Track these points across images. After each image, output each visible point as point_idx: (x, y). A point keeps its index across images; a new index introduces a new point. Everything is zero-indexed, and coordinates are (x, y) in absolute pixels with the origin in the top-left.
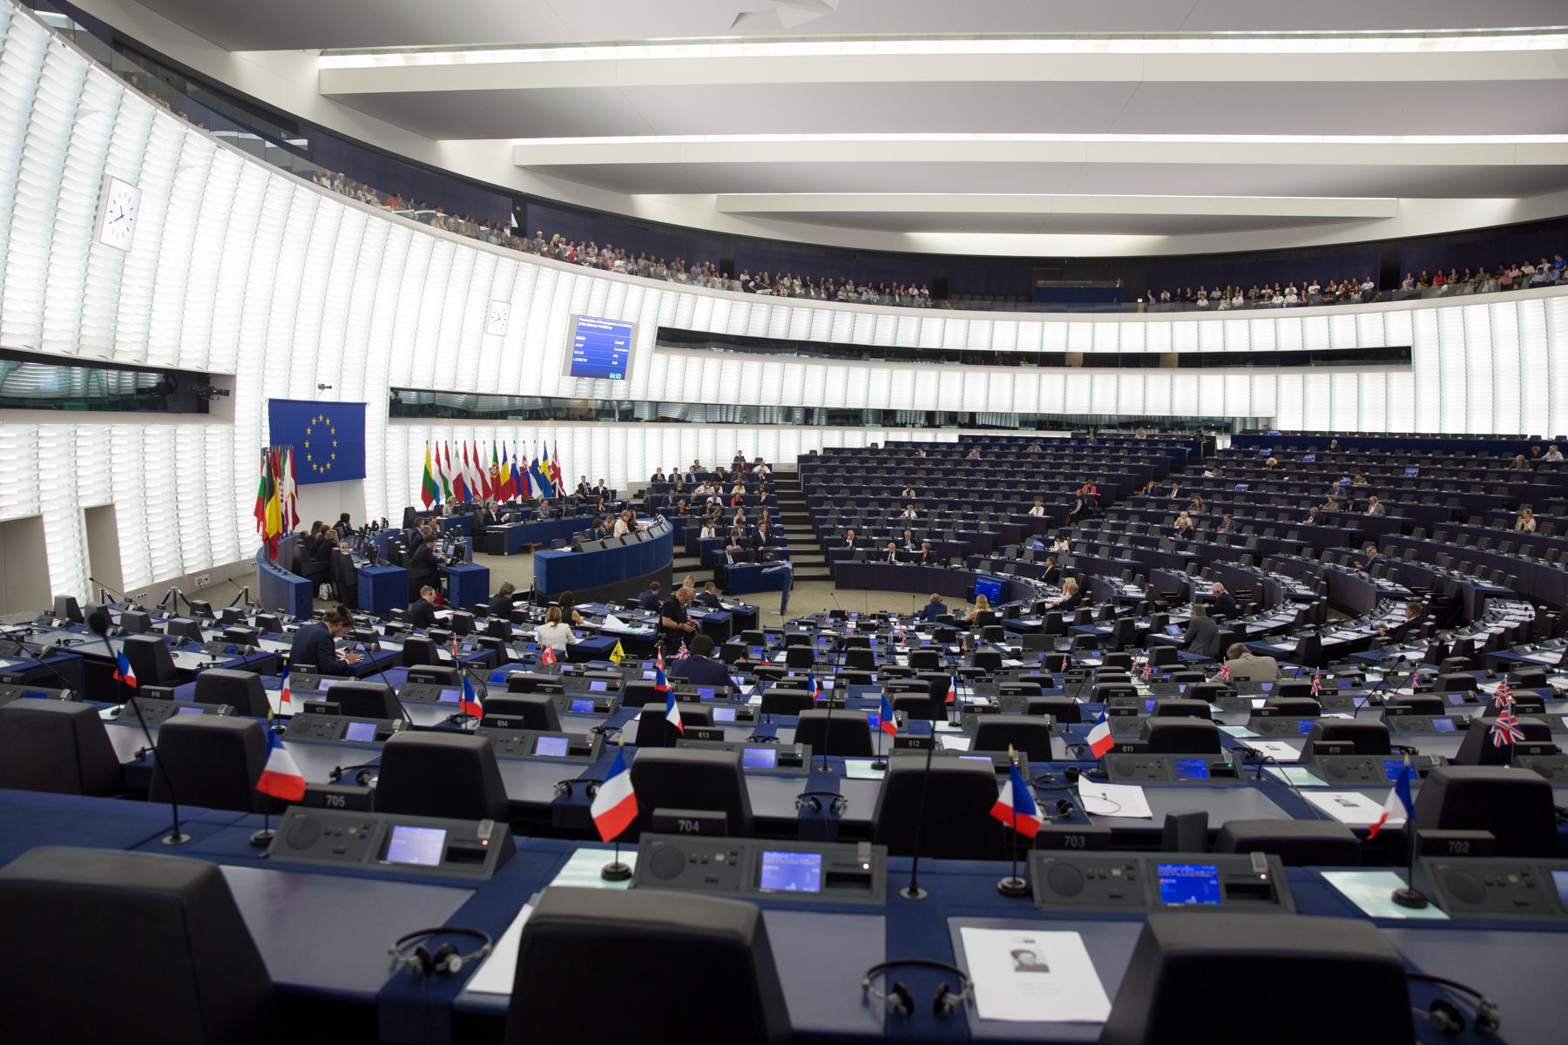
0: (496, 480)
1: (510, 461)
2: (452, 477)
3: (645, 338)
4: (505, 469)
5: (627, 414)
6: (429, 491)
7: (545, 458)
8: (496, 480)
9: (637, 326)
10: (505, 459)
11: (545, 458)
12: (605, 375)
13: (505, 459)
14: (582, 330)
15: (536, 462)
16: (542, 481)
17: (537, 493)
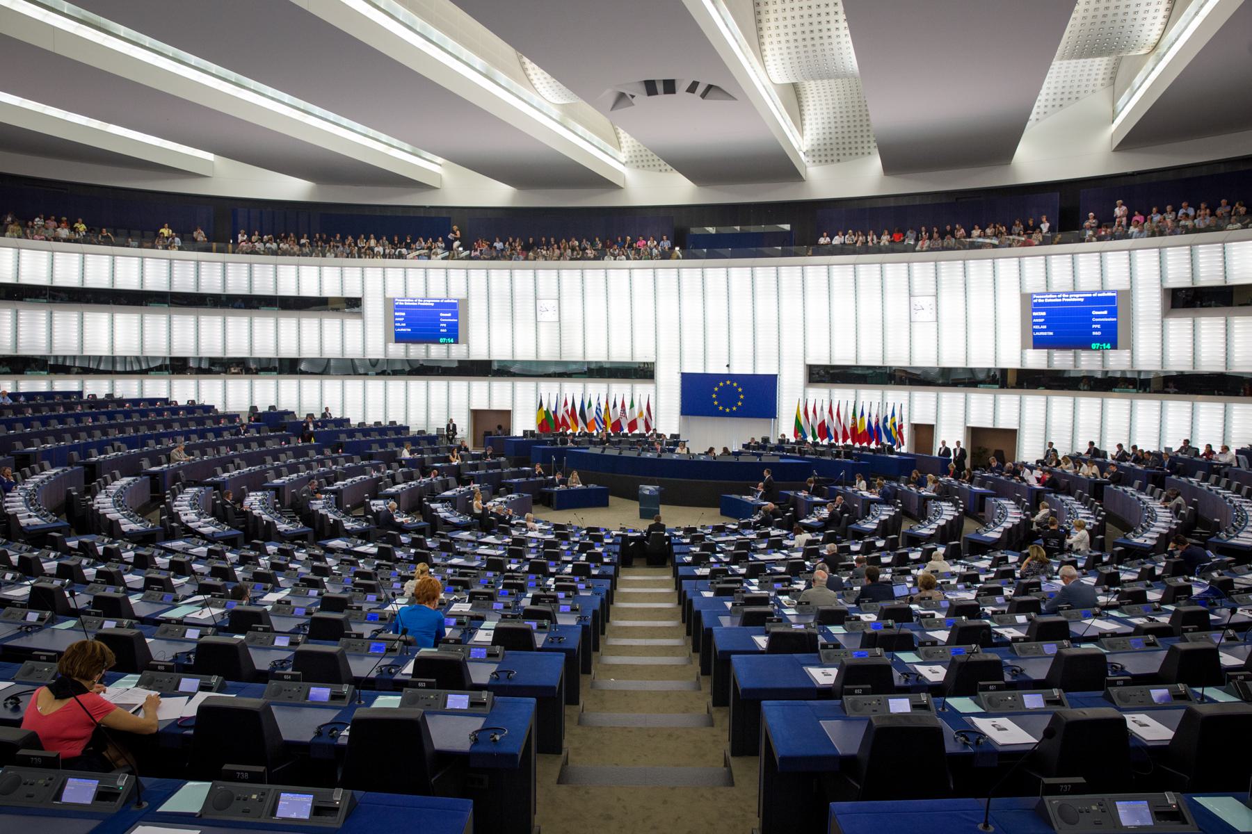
0: (854, 429)
1: (866, 415)
2: (818, 422)
3: (1147, 303)
4: (862, 421)
5: (1105, 384)
6: (798, 429)
7: (893, 415)
8: (854, 429)
9: (1127, 295)
10: (862, 414)
11: (893, 415)
12: (1086, 346)
13: (862, 414)
14: (1038, 306)
15: (886, 419)
16: (888, 433)
17: (884, 440)
